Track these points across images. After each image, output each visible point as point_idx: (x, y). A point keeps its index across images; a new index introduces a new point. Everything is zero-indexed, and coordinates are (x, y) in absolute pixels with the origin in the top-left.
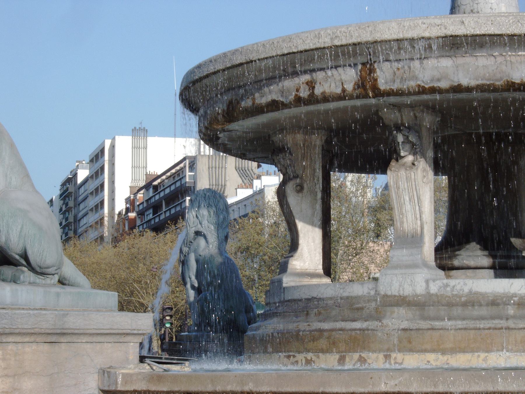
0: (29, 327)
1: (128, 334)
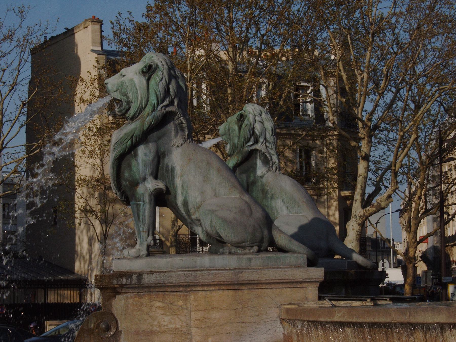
0: (210, 281)
1: (301, 282)
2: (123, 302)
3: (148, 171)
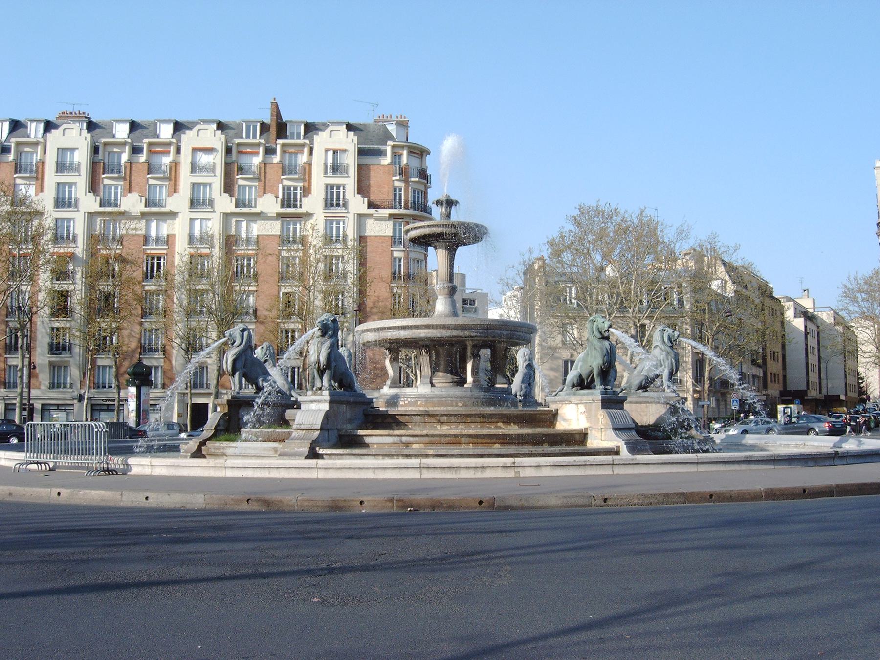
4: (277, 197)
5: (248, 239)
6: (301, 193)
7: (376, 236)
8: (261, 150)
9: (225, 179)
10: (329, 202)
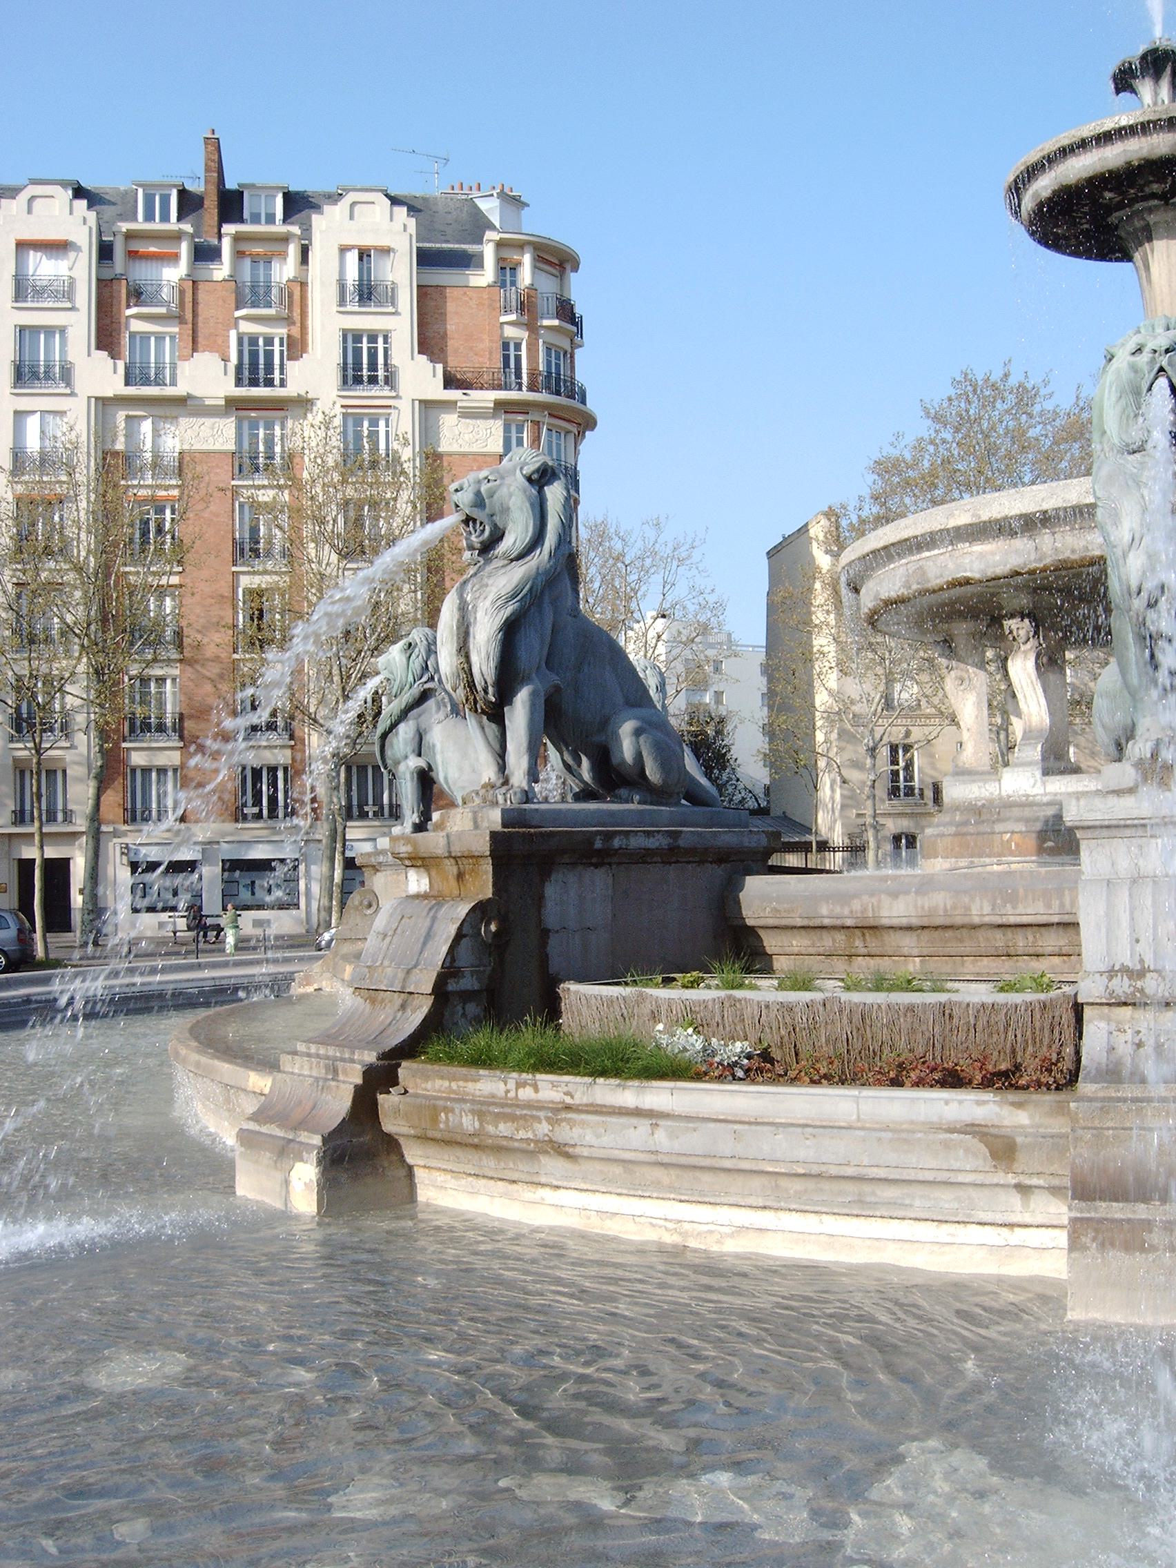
2: (383, 880)
3: (409, 749)
4: (225, 360)
5: (156, 464)
6: (282, 352)
7: (464, 455)
8: (184, 249)
9: (98, 319)
10: (350, 372)
